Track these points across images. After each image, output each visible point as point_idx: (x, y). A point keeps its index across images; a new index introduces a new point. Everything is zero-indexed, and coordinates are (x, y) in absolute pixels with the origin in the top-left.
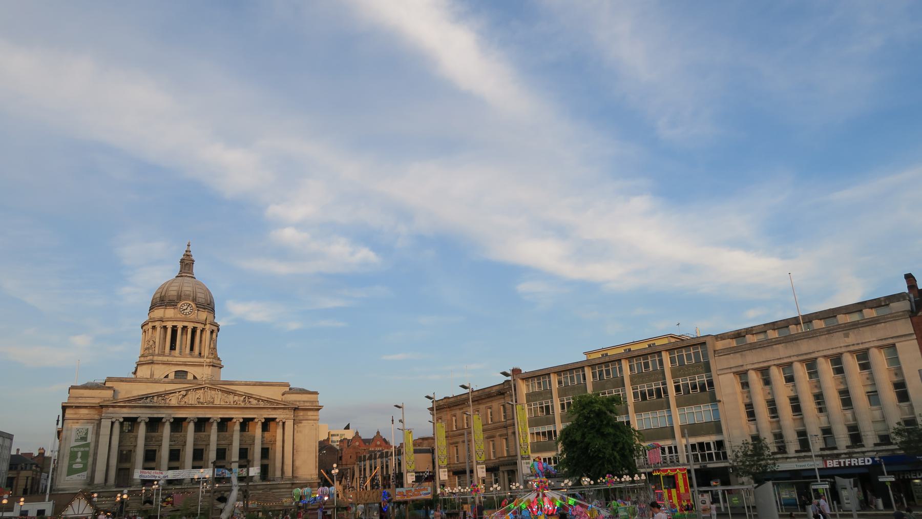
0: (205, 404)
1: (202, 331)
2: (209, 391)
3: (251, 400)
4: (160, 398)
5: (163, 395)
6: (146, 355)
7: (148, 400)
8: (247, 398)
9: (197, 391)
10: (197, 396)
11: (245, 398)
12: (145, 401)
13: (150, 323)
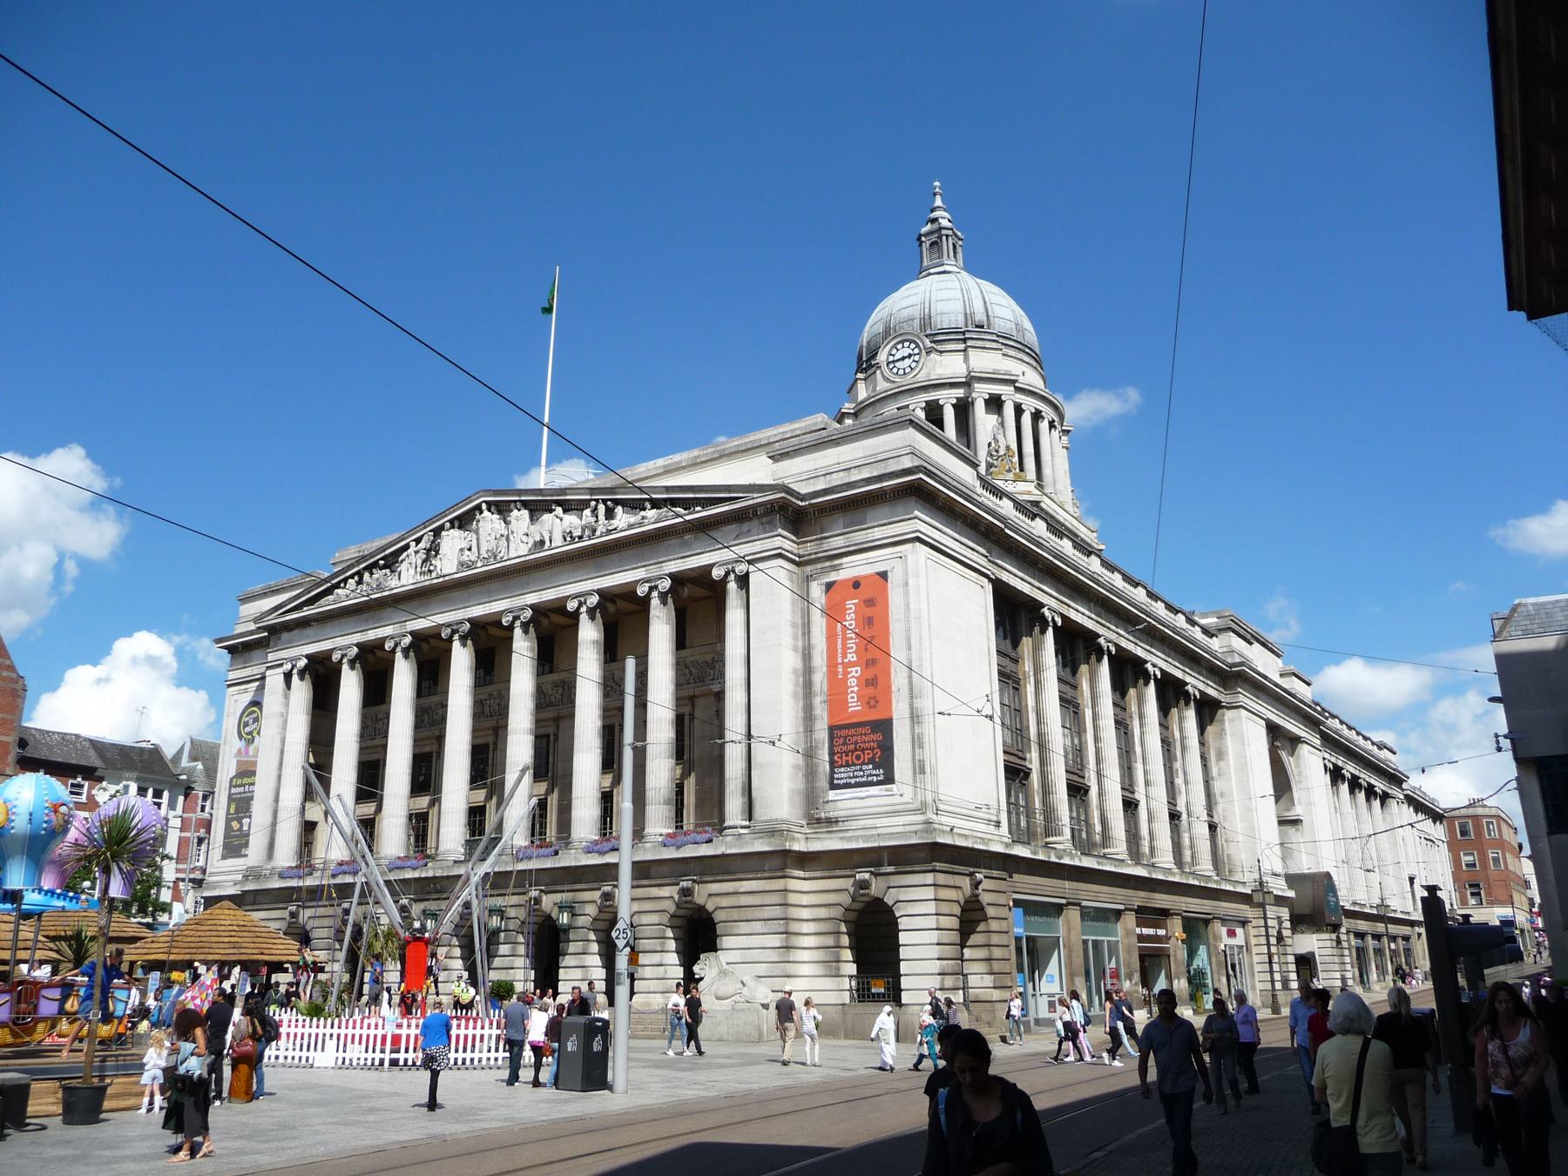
1: (963, 409)
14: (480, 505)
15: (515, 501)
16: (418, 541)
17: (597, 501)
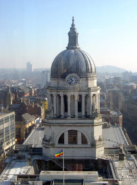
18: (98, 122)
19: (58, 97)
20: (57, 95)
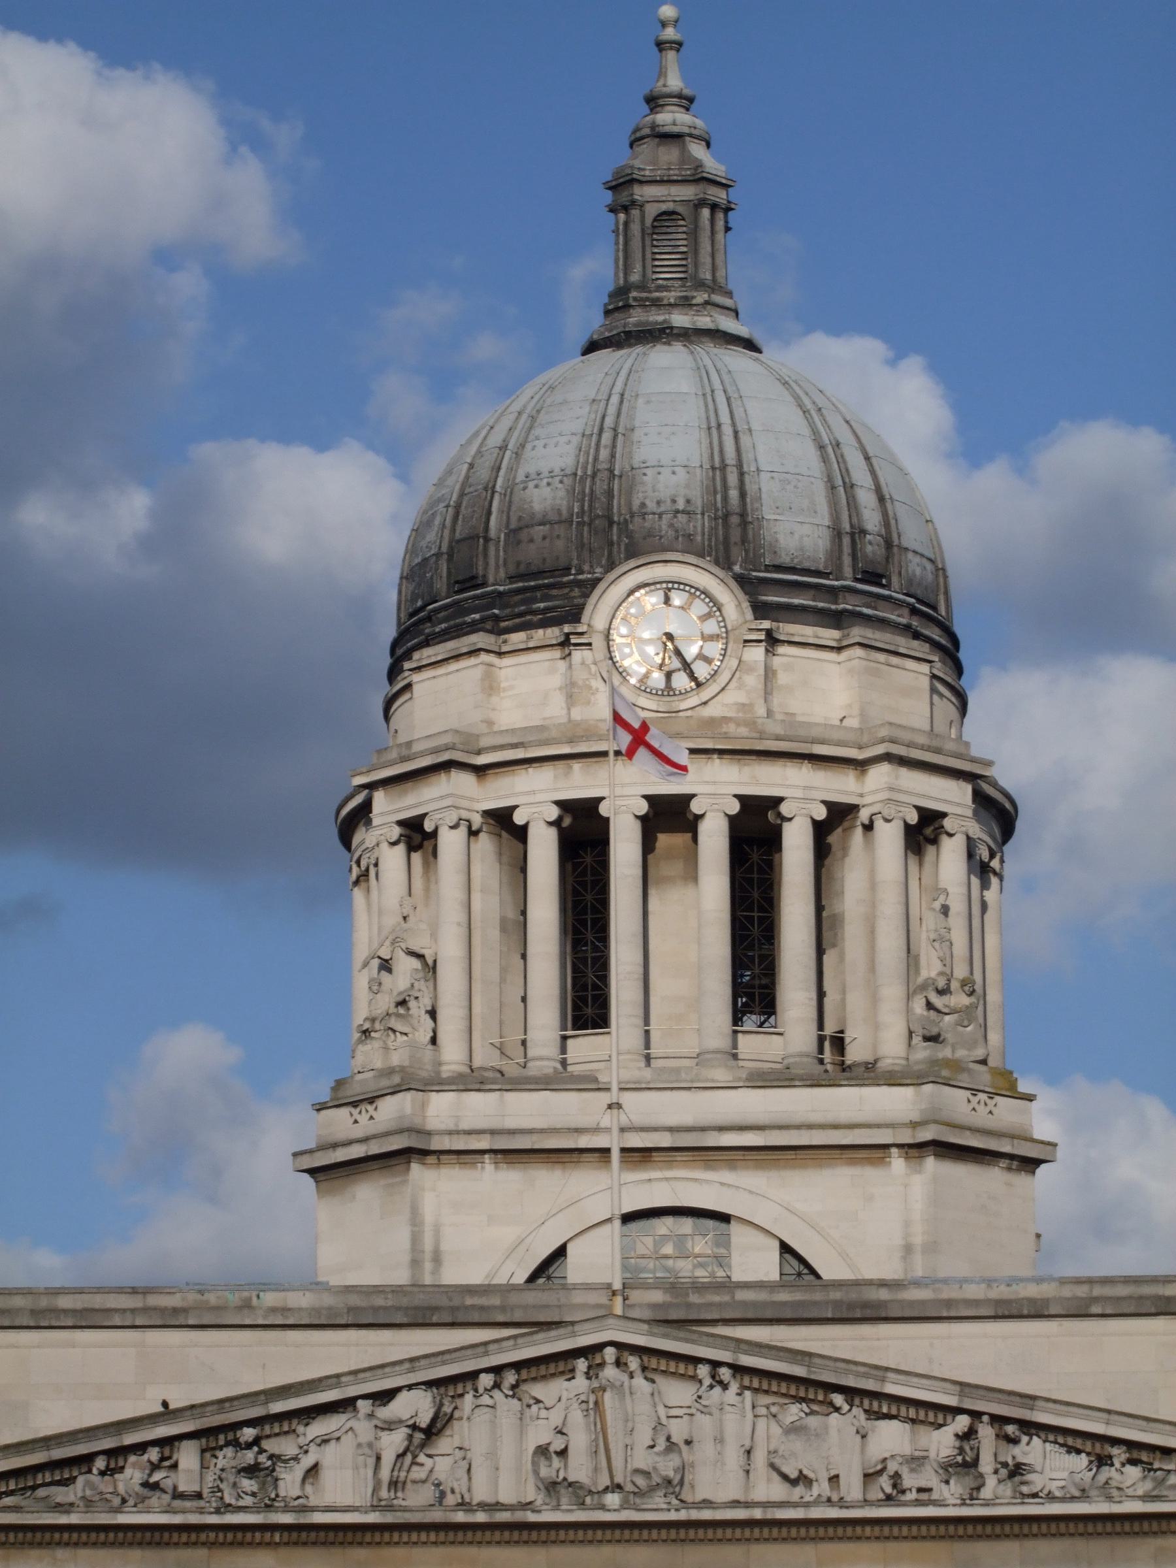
0: (613, 1499)
2: (639, 1381)
3: (1032, 1450)
4: (226, 1458)
5: (248, 1433)
6: (363, 1083)
7: (132, 1475)
8: (986, 1432)
9: (538, 1390)
10: (541, 1433)
11: (969, 1435)
12: (105, 1485)
13: (380, 800)
14: (599, 1347)
15: (715, 1364)
16: (385, 1397)
17: (976, 1415)
18: (981, 1118)
19: (485, 844)
20: (477, 820)
